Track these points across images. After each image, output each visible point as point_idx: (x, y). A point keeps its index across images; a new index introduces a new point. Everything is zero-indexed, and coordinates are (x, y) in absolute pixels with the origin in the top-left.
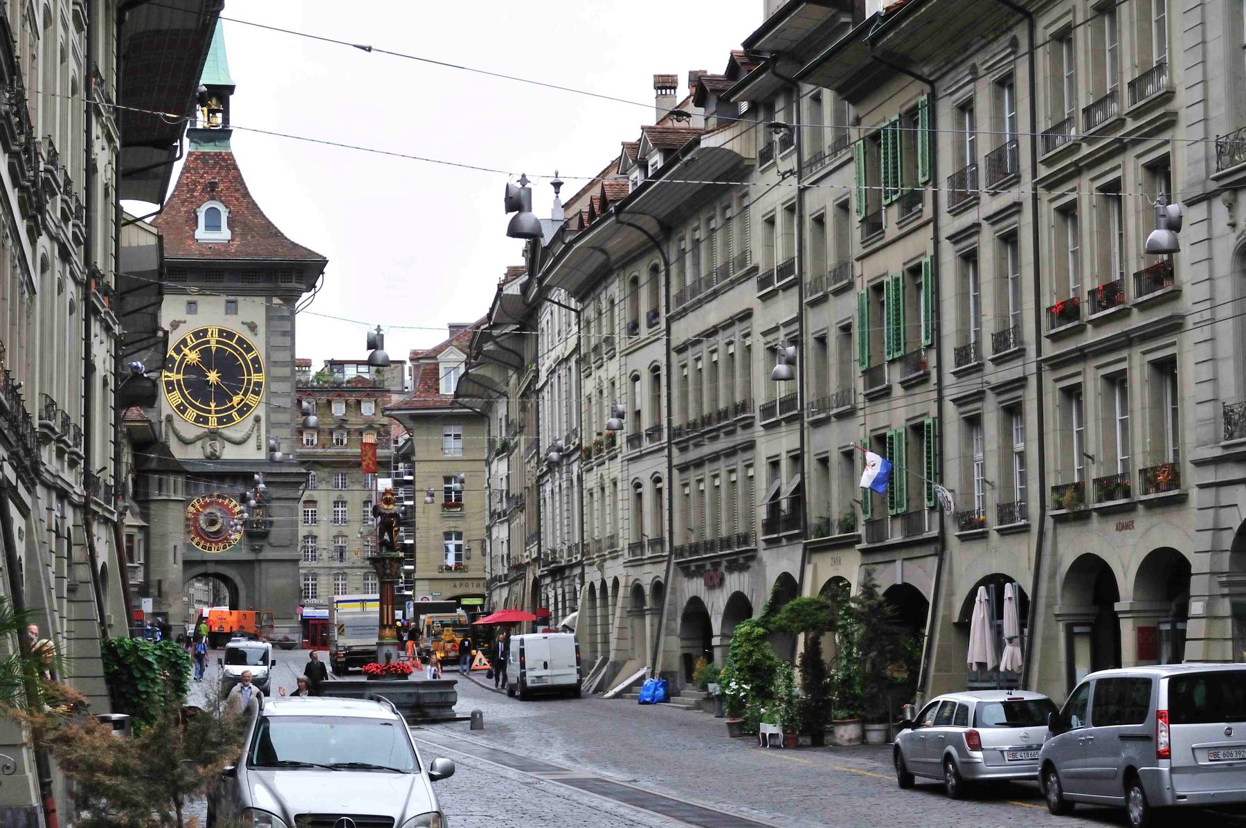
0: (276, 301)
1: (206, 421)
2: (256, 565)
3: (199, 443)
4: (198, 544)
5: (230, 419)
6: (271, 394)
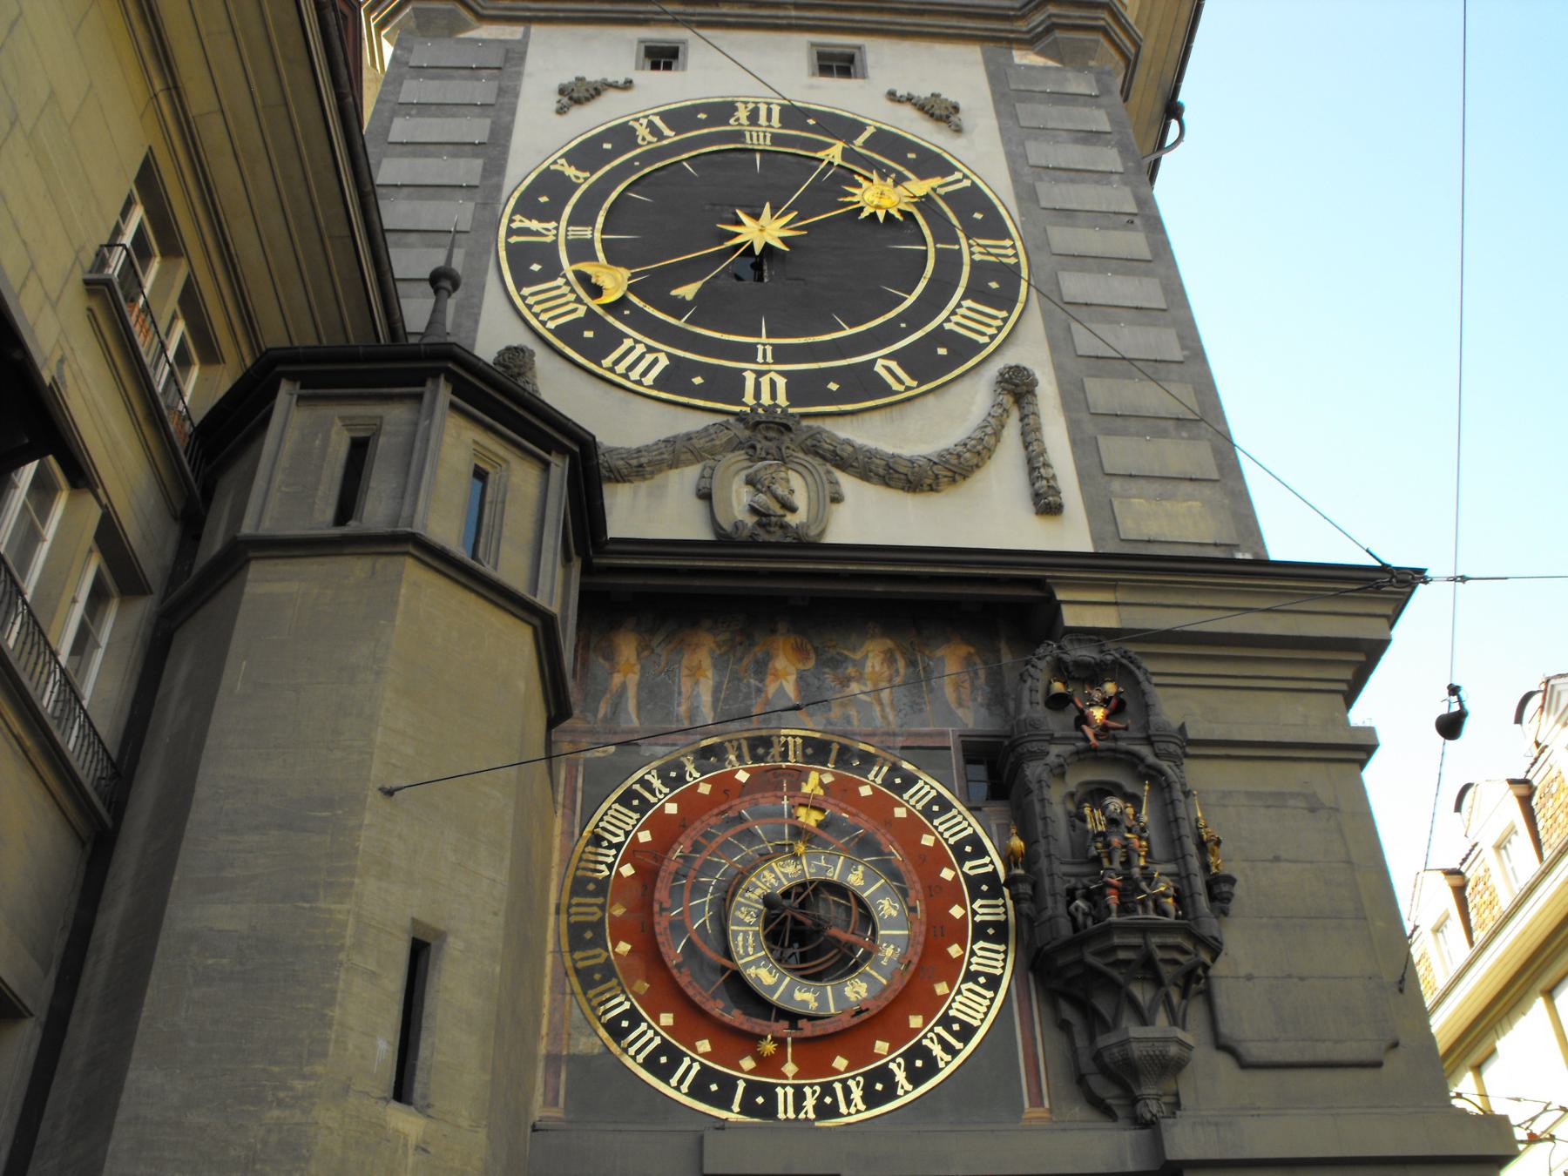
0: (1025, 58)
1: (727, 386)
3: (684, 479)
4: (663, 1062)
5: (864, 385)
6: (1064, 314)
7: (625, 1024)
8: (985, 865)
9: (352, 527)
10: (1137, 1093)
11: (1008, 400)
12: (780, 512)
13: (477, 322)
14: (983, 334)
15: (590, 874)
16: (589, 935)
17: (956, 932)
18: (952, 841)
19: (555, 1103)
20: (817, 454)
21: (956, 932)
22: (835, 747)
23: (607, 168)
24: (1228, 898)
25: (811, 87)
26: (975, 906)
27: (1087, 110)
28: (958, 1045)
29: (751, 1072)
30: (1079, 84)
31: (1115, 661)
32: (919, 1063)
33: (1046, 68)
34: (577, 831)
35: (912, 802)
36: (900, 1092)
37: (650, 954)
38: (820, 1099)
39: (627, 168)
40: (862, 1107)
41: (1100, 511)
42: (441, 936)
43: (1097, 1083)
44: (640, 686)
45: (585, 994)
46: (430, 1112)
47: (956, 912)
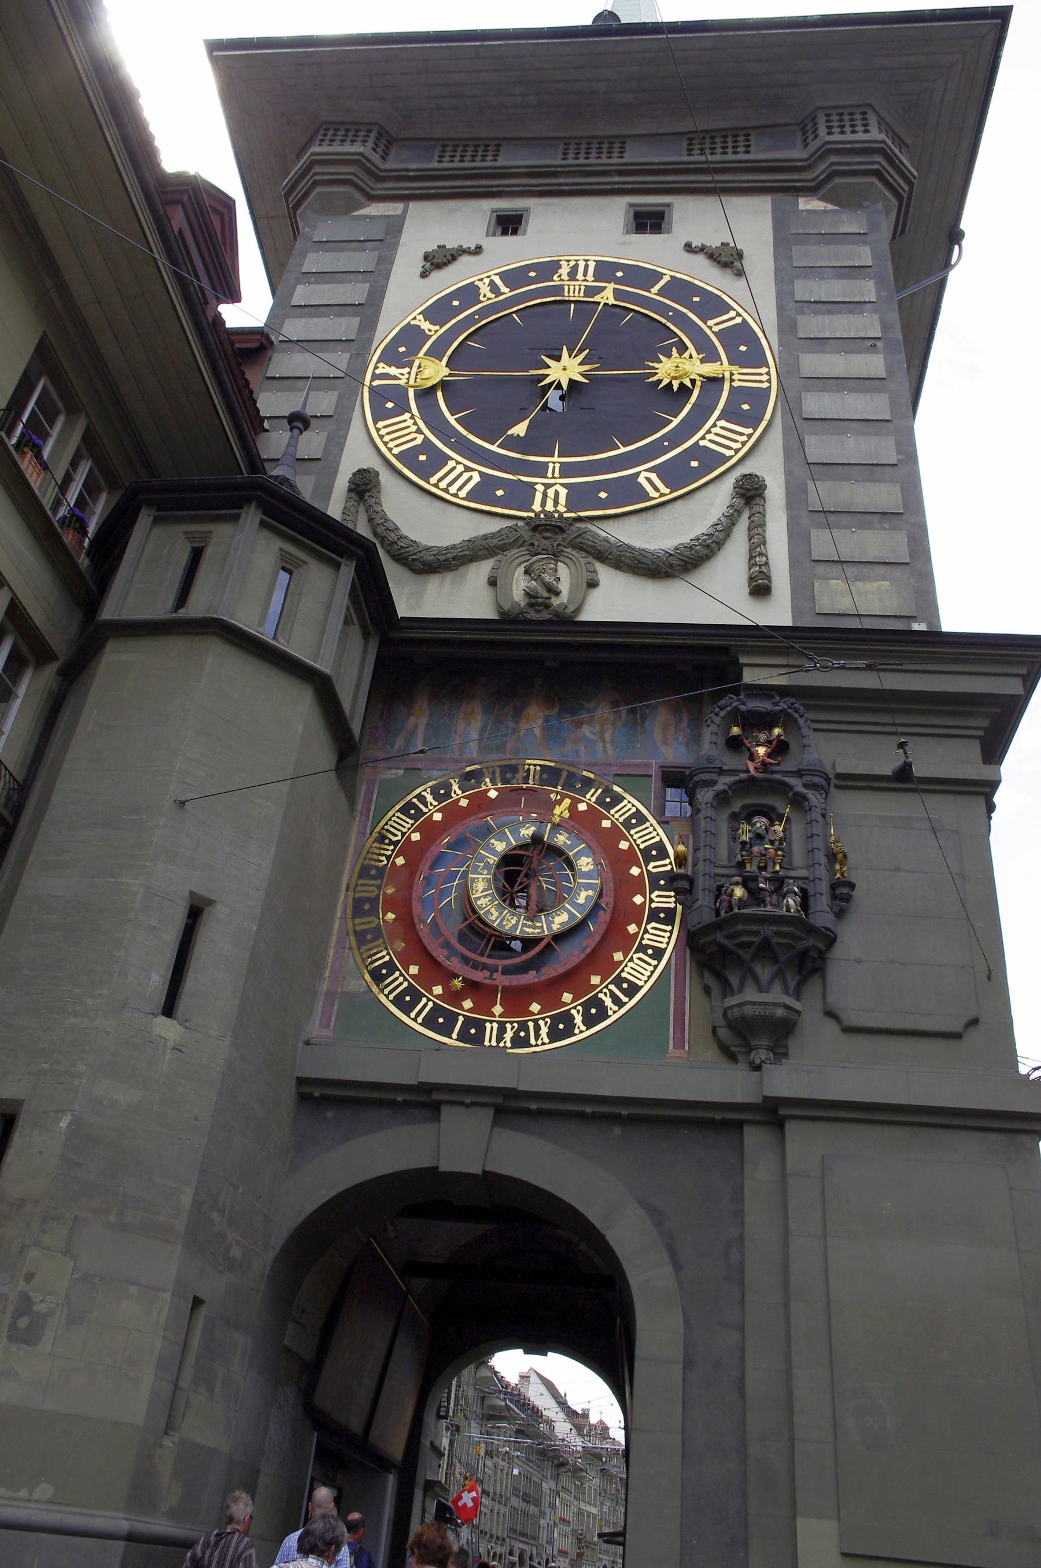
2: (754, 1138)
3: (480, 572)
4: (406, 1001)
7: (384, 971)
8: (666, 865)
9: (182, 613)
10: (753, 1044)
11: (739, 502)
12: (546, 595)
13: (342, 450)
14: (729, 448)
15: (374, 863)
16: (367, 907)
17: (636, 914)
18: (642, 846)
19: (329, 1026)
20: (582, 549)
21: (636, 914)
22: (565, 774)
23: (454, 321)
24: (848, 898)
25: (624, 244)
26: (653, 896)
27: (853, 247)
28: (625, 999)
29: (468, 1011)
30: (851, 224)
31: (783, 711)
32: (593, 1011)
33: (825, 212)
34: (368, 832)
35: (617, 816)
36: (577, 1031)
37: (407, 922)
38: (516, 1033)
39: (469, 320)
40: (546, 1040)
41: (801, 590)
42: (211, 903)
43: (724, 1033)
44: (428, 724)
45: (359, 949)
46: (187, 1024)
47: (638, 899)
